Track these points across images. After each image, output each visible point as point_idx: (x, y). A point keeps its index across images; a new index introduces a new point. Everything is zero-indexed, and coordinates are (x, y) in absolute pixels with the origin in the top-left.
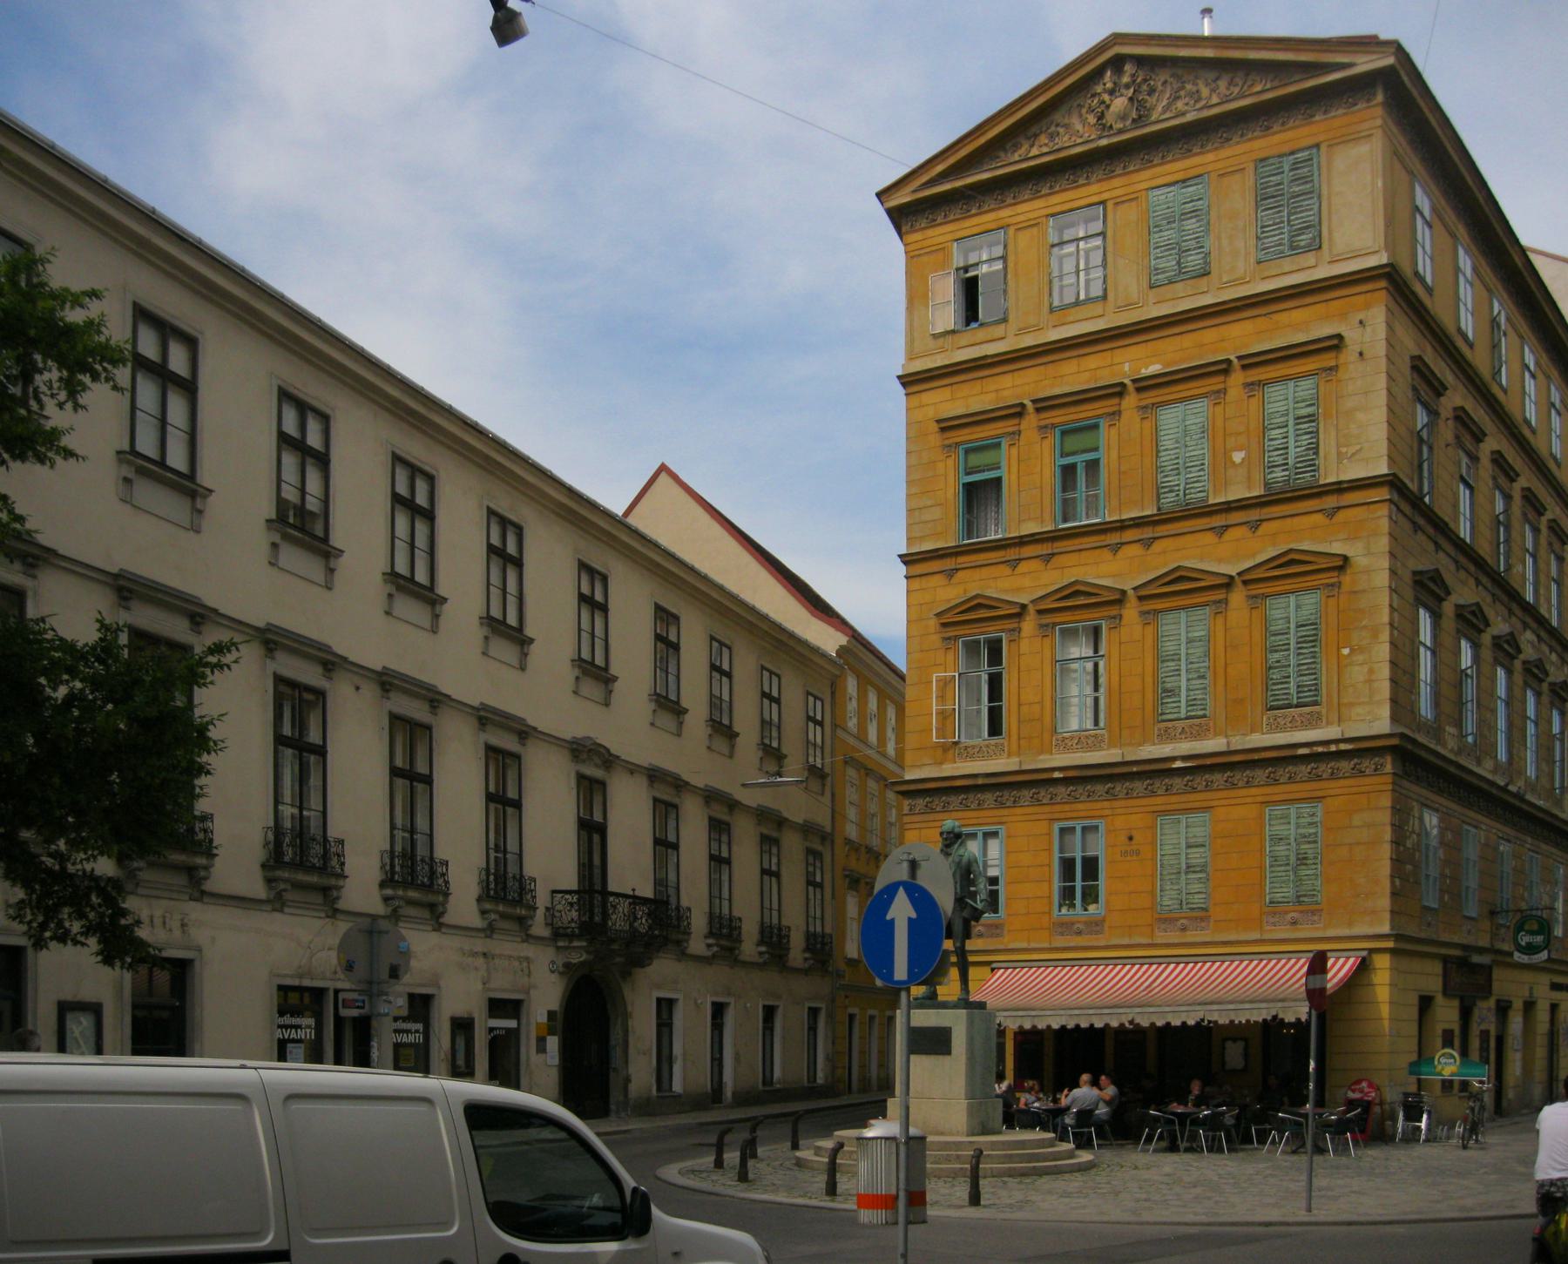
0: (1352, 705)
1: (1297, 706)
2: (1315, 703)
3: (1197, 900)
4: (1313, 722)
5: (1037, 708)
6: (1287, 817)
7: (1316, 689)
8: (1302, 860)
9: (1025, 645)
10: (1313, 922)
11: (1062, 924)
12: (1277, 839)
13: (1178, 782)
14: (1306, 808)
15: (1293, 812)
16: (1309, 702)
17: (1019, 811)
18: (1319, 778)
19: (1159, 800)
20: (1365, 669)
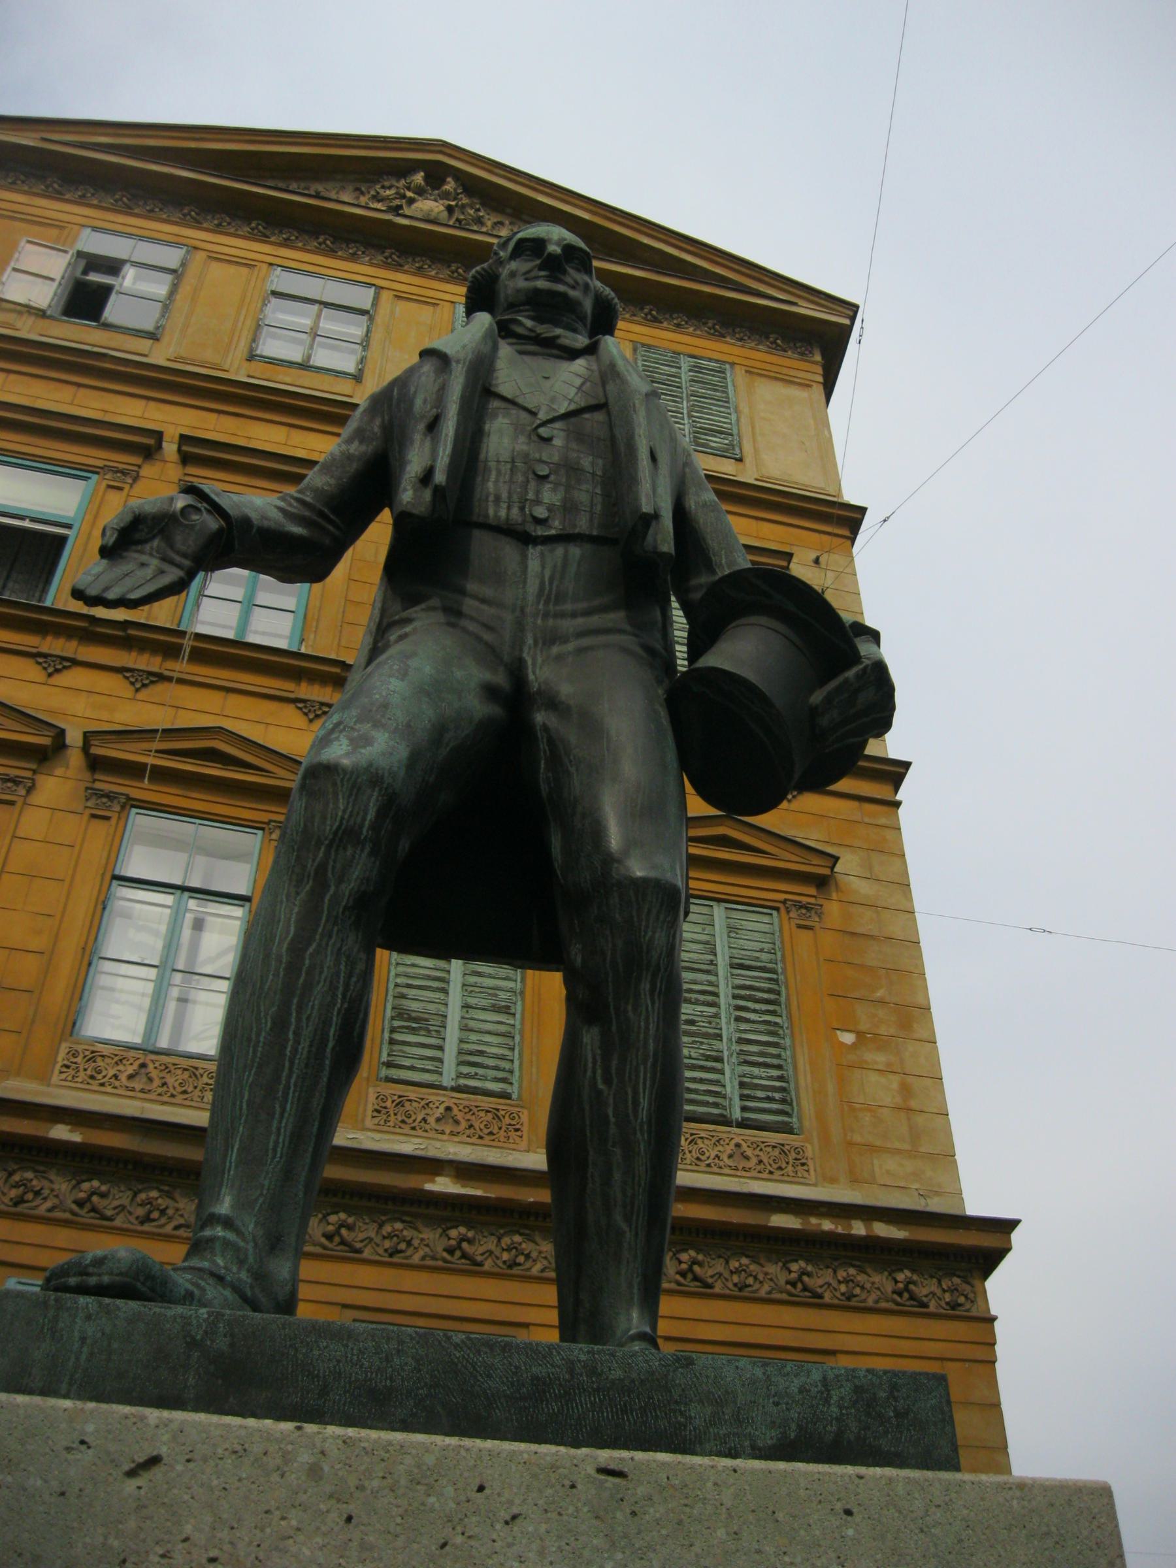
0: (873, 1149)
1: (743, 1124)
2: (787, 1129)
7: (785, 1098)
13: (429, 1239)
18: (814, 1300)
19: (366, 1275)
20: (894, 1082)
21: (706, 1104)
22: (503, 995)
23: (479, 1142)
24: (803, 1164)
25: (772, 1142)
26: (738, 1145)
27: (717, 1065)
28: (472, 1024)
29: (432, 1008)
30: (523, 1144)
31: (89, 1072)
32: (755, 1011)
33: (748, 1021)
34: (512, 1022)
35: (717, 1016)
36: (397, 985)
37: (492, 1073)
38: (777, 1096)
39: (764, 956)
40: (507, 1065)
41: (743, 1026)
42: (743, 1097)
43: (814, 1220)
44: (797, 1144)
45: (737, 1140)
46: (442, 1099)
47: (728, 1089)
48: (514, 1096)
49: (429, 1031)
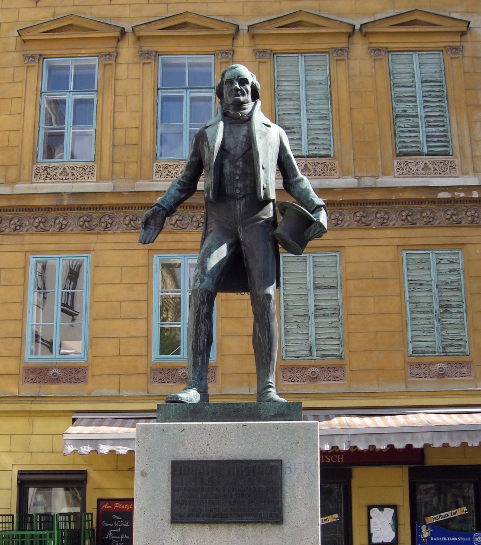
1: (427, 155)
2: (446, 154)
3: (330, 346)
4: (449, 169)
5: (135, 133)
6: (428, 261)
8: (446, 308)
9: (122, 71)
10: (462, 375)
11: (162, 370)
12: (416, 285)
14: (446, 255)
15: (432, 257)
16: (440, 149)
17: (109, 238)
18: (458, 224)
21: (413, 147)
22: (324, 112)
23: (320, 177)
24: (454, 168)
25: (441, 160)
26: (425, 164)
27: (416, 129)
28: (312, 127)
29: (295, 123)
30: (337, 175)
31: (166, 173)
32: (433, 102)
33: (429, 106)
34: (328, 123)
35: (416, 106)
36: (279, 115)
37: (322, 147)
38: (443, 139)
39: (437, 75)
40: (328, 143)
41: (427, 110)
42: (428, 142)
43: (456, 194)
44: (451, 160)
45: (425, 161)
46: (303, 161)
47: (421, 139)
48: (332, 156)
49: (294, 132)
